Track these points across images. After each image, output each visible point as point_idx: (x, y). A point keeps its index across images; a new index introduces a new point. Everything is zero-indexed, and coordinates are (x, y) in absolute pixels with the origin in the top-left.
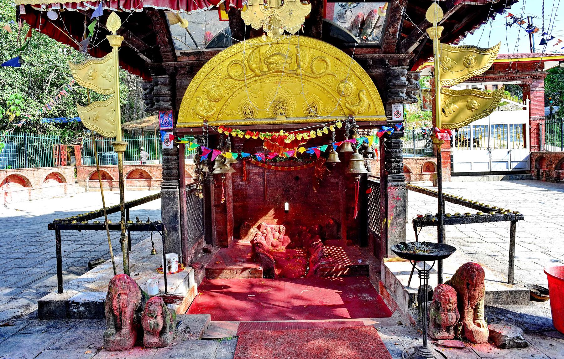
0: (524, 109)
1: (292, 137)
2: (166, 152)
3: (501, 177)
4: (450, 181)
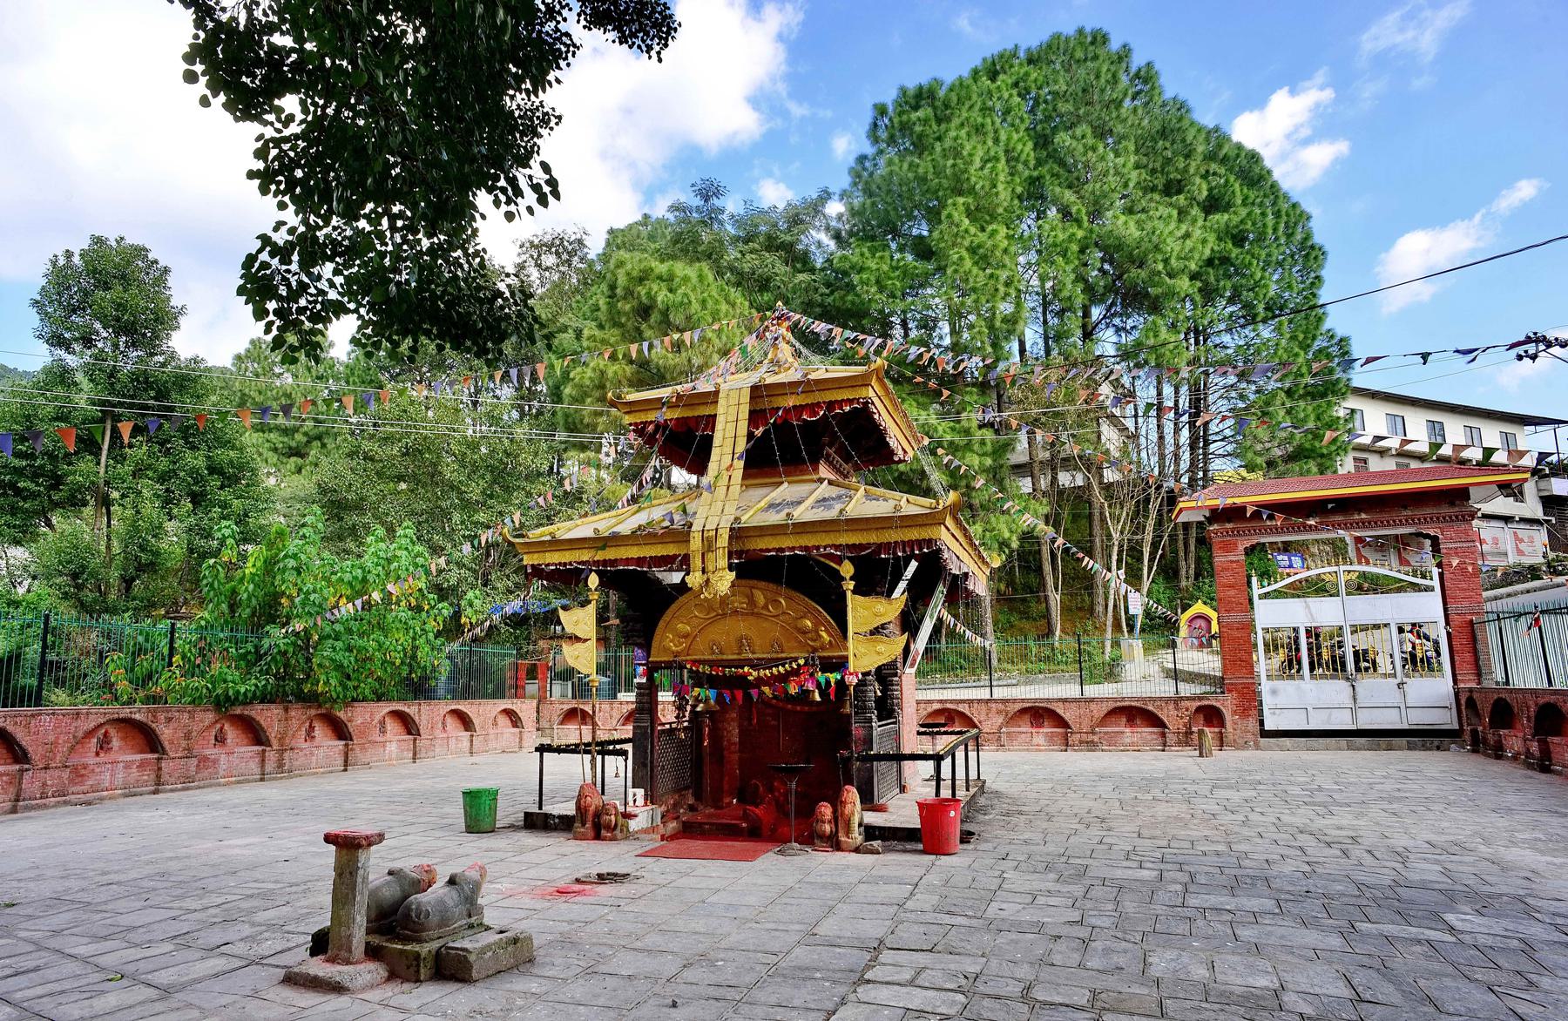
0: (1429, 589)
2: (640, 686)
4: (1257, 747)
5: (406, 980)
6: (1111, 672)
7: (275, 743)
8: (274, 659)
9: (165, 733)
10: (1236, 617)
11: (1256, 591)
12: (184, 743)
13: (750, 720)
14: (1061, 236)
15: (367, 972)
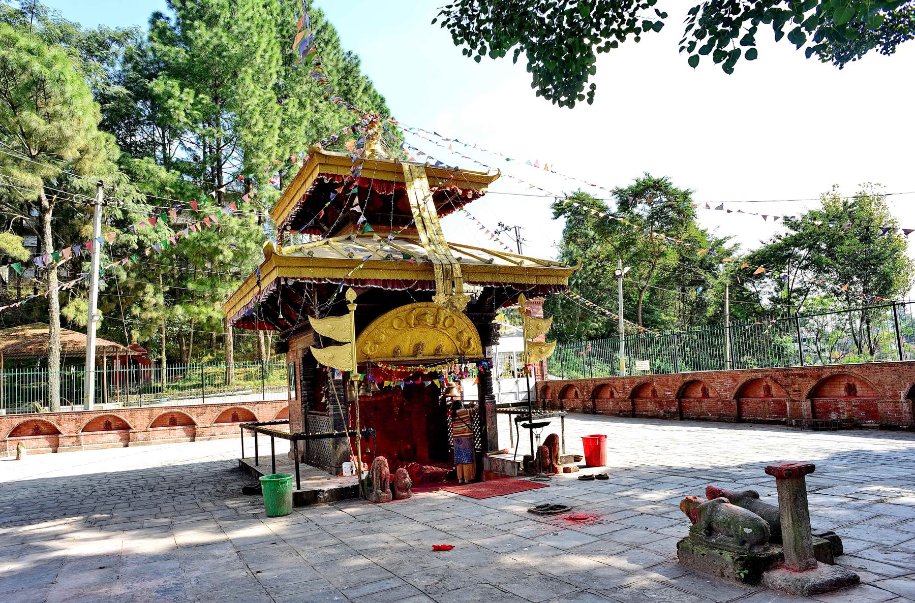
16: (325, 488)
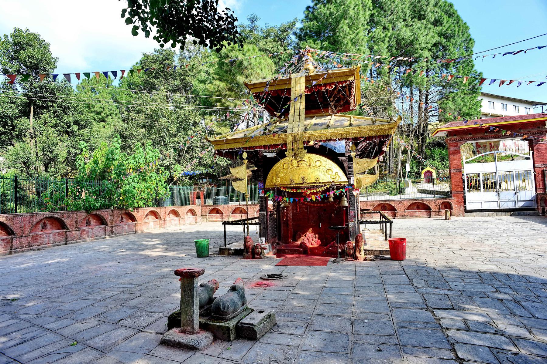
0: (529, 158)
1: (309, 192)
2: (261, 197)
3: (509, 213)
4: (464, 216)
5: (223, 340)
6: (401, 191)
7: (109, 224)
8: (107, 193)
9: (67, 222)
10: (457, 170)
11: (465, 161)
12: (75, 225)
13: (296, 210)
14: (383, 35)
15: (203, 338)
16: (233, 249)
